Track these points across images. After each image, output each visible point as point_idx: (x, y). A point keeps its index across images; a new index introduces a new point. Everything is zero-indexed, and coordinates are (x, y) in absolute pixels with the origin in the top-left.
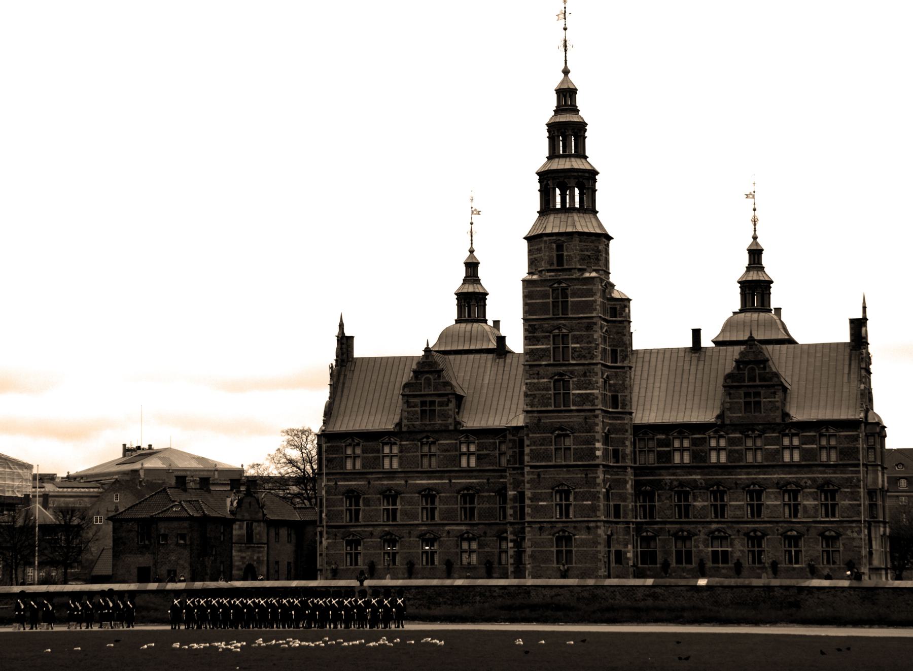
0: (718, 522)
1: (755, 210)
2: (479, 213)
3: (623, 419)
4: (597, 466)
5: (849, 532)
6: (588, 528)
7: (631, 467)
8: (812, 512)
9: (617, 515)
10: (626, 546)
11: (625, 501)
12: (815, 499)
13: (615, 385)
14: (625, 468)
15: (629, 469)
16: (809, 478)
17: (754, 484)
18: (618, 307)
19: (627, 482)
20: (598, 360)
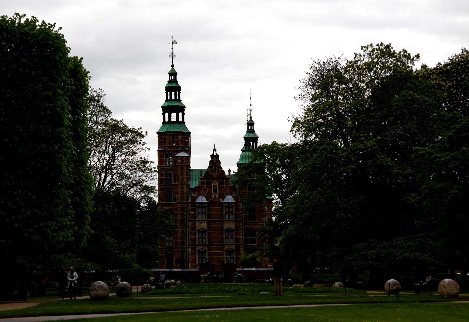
1: (251, 105)
3: (177, 206)
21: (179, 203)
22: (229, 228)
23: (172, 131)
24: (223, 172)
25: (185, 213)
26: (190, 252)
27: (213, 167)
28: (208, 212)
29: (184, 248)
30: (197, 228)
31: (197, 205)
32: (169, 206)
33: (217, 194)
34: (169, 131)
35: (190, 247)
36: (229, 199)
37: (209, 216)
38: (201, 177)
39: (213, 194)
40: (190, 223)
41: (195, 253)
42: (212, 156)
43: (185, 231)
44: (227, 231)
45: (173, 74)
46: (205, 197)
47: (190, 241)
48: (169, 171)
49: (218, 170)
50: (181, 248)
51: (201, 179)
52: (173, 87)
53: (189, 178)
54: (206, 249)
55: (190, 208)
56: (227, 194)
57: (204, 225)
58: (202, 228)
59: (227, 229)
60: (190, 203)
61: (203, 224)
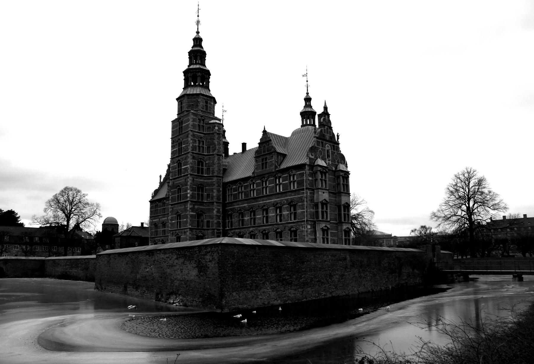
0: (253, 227)
2: (226, 111)
3: (213, 179)
4: (188, 201)
5: (301, 228)
6: (185, 232)
7: (216, 202)
8: (286, 218)
9: (208, 226)
12: (288, 211)
13: (209, 163)
14: (213, 203)
15: (215, 203)
16: (285, 200)
17: (265, 206)
19: (214, 210)
20: (190, 150)
21: (217, 176)
22: (347, 203)
25: (221, 189)
27: (326, 127)
29: (219, 230)
32: (201, 179)
39: (327, 159)
43: (221, 210)
45: (198, 41)
48: (201, 138)
50: (218, 230)
52: (197, 54)
54: (329, 226)
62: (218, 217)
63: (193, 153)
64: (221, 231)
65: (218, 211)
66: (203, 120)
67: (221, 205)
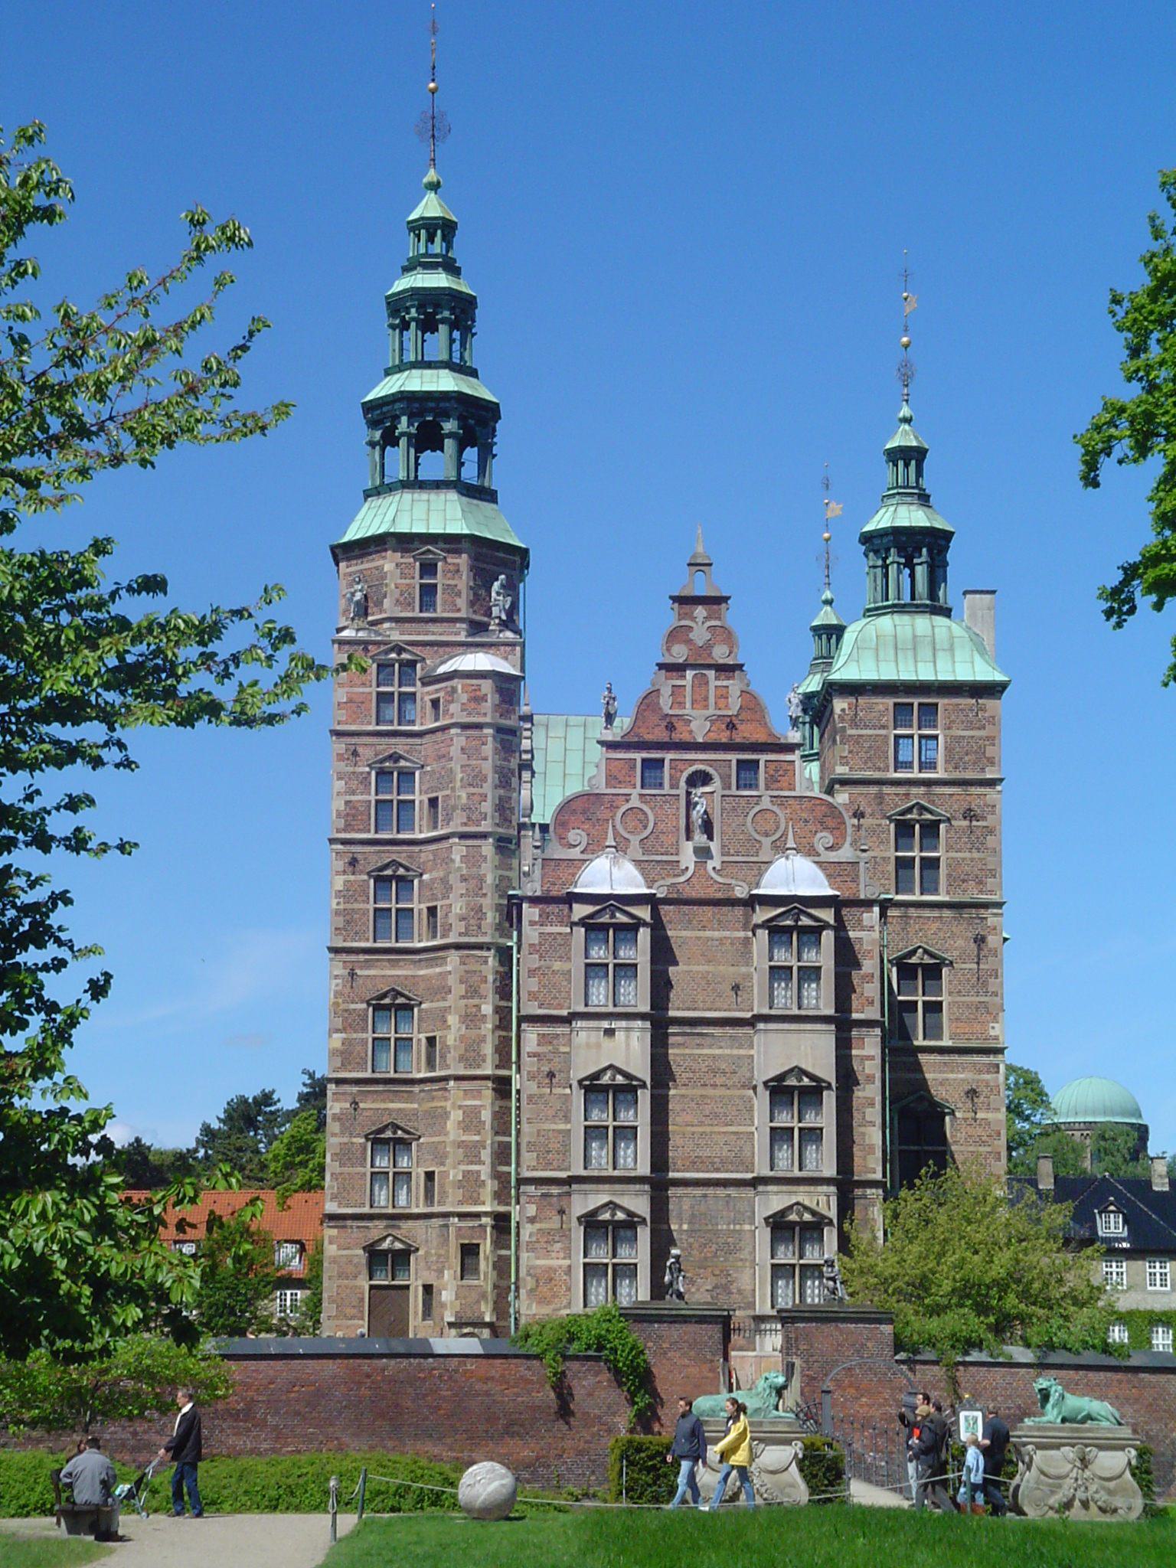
10: (440, 1272)
11: (443, 1164)
14: (446, 1079)
18: (441, 694)
19: (446, 1115)
21: (458, 947)
23: (419, 528)
24: (752, 705)
25: (487, 1009)
26: (527, 1231)
27: (689, 674)
28: (653, 961)
29: (477, 1215)
30: (582, 1068)
31: (581, 911)
32: (394, 964)
33: (714, 846)
34: (403, 527)
35: (531, 1189)
36: (795, 875)
37: (661, 987)
38: (609, 736)
40: (531, 1036)
41: (564, 1234)
42: (684, 601)
43: (486, 1115)
44: (780, 1091)
46: (637, 863)
47: (528, 1158)
48: (395, 757)
49: (723, 695)
50: (462, 1216)
51: (610, 746)
53: (527, 766)
55: (531, 934)
56: (780, 848)
57: (630, 1051)
58: (611, 1067)
59: (781, 1077)
60: (534, 901)
61: (620, 1035)
62: (471, 1153)
63: (345, 842)
64: (487, 1221)
65: (470, 1120)
66: (412, 664)
67: (487, 1091)
